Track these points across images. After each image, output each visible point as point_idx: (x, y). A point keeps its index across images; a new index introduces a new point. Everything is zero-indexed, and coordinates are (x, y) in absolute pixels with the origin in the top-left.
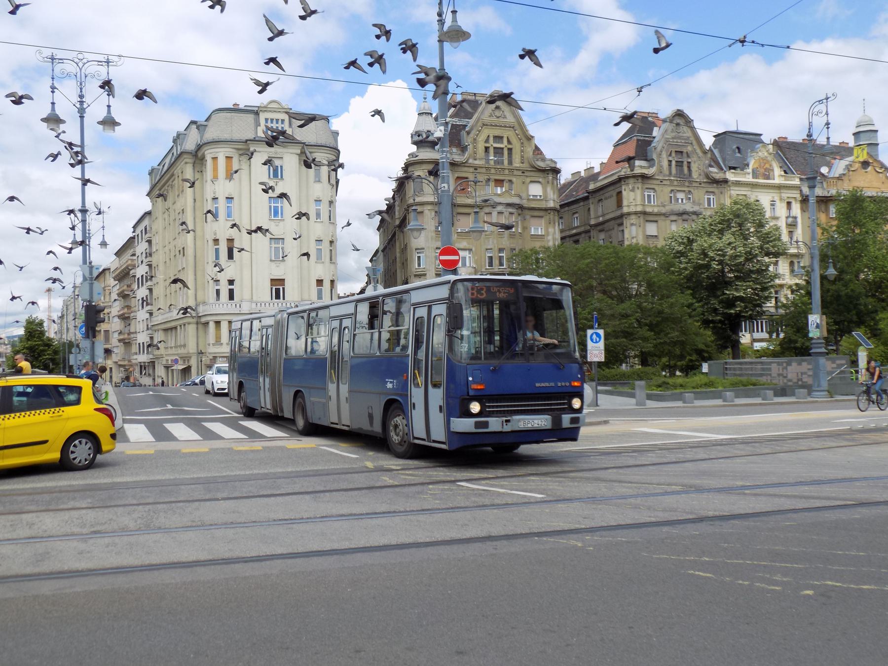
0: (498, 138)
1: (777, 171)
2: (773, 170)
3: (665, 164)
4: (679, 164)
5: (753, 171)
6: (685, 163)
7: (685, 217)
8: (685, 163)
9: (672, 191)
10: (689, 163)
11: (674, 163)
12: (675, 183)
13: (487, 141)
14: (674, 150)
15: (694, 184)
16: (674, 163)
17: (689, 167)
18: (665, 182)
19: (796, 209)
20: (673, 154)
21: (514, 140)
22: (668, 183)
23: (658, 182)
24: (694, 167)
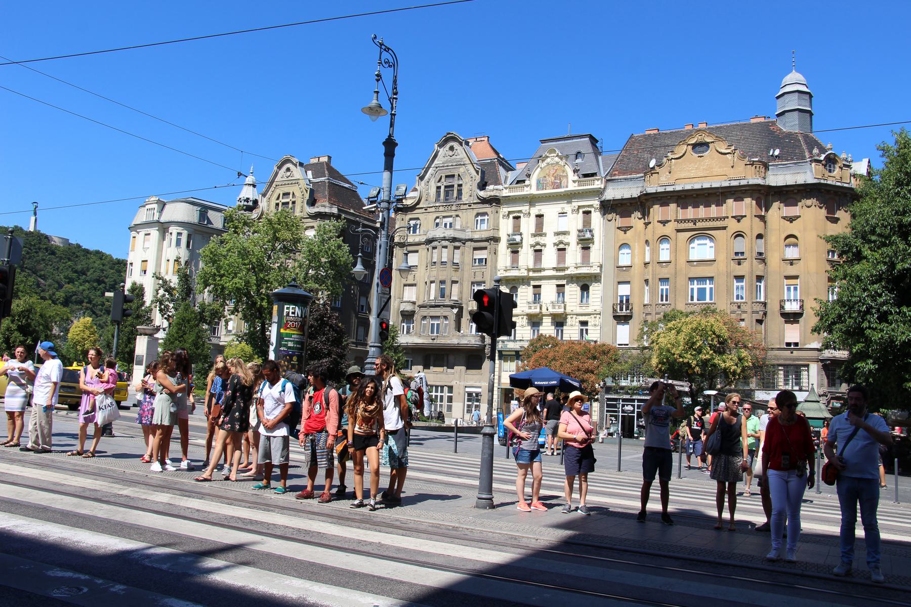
0: (286, 194)
1: (572, 176)
2: (567, 176)
3: (433, 191)
4: (449, 187)
5: (538, 182)
6: (456, 186)
7: (435, 244)
8: (456, 186)
9: (437, 217)
10: (460, 185)
11: (443, 188)
12: (441, 209)
13: (278, 198)
14: (444, 175)
15: (462, 207)
16: (443, 188)
18: (429, 210)
21: (298, 194)
23: (423, 210)
24: (465, 190)
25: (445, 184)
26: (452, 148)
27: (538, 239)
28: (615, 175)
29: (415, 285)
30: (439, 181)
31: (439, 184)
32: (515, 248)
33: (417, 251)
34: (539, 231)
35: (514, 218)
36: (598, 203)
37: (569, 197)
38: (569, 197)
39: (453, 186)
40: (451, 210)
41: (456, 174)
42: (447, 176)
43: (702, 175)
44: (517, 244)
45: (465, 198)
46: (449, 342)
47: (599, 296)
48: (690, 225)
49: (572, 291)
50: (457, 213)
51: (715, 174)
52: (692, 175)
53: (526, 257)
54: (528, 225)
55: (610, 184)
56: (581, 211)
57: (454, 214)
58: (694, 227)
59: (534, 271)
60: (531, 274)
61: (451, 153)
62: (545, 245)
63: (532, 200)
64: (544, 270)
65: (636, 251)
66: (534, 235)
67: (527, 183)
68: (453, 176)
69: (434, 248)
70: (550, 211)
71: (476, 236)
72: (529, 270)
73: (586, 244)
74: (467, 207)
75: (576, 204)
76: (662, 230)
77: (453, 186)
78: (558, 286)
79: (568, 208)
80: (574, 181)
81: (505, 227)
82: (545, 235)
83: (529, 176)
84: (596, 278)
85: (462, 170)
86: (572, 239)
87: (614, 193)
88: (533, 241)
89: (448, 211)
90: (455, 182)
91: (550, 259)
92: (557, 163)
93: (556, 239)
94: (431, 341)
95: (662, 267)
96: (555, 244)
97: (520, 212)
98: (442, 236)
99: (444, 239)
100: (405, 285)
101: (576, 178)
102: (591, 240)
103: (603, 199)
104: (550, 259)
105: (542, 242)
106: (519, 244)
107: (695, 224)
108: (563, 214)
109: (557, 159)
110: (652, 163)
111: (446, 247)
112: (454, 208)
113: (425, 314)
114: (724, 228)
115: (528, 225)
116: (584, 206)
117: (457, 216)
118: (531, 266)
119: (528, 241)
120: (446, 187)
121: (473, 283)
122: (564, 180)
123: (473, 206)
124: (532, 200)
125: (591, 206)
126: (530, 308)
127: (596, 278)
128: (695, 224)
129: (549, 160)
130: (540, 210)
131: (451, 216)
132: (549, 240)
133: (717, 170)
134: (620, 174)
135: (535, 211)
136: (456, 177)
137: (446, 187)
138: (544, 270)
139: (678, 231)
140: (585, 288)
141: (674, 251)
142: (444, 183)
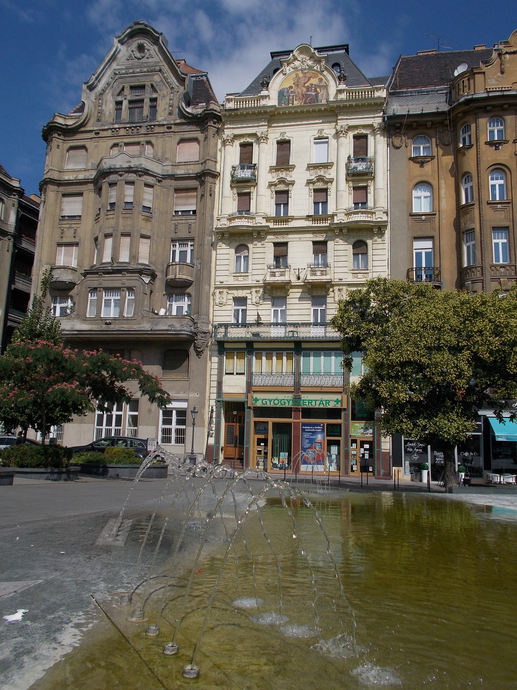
1: (333, 87)
2: (326, 87)
3: (109, 107)
5: (281, 94)
6: (147, 101)
8: (147, 101)
10: (154, 100)
11: (125, 103)
12: (122, 132)
15: (157, 130)
16: (125, 103)
17: (153, 108)
18: (102, 134)
19: (379, 147)
20: (127, 91)
22: (109, 133)
23: (93, 135)
24: (162, 106)
25: (129, 98)
26: (141, 48)
27: (283, 175)
29: (77, 244)
30: (118, 95)
31: (119, 99)
32: (244, 187)
33: (80, 194)
34: (283, 163)
35: (242, 145)
36: (380, 120)
37: (331, 112)
39: (142, 101)
40: (139, 134)
41: (148, 84)
42: (132, 88)
45: (161, 117)
46: (136, 327)
47: (386, 258)
49: (340, 250)
50: (147, 139)
53: (263, 203)
56: (351, 134)
57: (142, 139)
59: (276, 220)
60: (271, 225)
61: (138, 55)
62: (292, 183)
64: (293, 218)
66: (273, 169)
68: (143, 87)
69: (112, 184)
70: (302, 136)
71: (180, 171)
73: (360, 180)
74: (165, 129)
75: (344, 122)
76: (490, 156)
77: (142, 101)
78: (315, 243)
79: (329, 129)
81: (228, 158)
82: (293, 167)
84: (378, 229)
85: (157, 78)
86: (338, 175)
88: (274, 178)
89: (132, 136)
90: (147, 96)
91: (301, 203)
92: (311, 68)
93: (312, 175)
94: (104, 327)
95: (496, 210)
96: (309, 182)
97: (255, 135)
98: (126, 165)
99: (129, 170)
100: (60, 245)
102: (369, 175)
103: (390, 113)
104: (301, 203)
105: (289, 179)
106: (252, 181)
108: (321, 139)
109: (310, 63)
111: (132, 183)
112: (143, 131)
113: (95, 284)
115: (265, 155)
116: (356, 127)
117: (149, 143)
118: (272, 212)
119: (265, 177)
120: (130, 102)
121: (173, 241)
122: (321, 93)
123: (174, 128)
124: (272, 116)
125: (371, 126)
126: (273, 274)
127: (378, 229)
129: (297, 63)
130: (283, 134)
131: (138, 143)
132: (300, 176)
136: (148, 89)
137: (130, 102)
138: (293, 218)
140: (360, 248)
142: (129, 95)
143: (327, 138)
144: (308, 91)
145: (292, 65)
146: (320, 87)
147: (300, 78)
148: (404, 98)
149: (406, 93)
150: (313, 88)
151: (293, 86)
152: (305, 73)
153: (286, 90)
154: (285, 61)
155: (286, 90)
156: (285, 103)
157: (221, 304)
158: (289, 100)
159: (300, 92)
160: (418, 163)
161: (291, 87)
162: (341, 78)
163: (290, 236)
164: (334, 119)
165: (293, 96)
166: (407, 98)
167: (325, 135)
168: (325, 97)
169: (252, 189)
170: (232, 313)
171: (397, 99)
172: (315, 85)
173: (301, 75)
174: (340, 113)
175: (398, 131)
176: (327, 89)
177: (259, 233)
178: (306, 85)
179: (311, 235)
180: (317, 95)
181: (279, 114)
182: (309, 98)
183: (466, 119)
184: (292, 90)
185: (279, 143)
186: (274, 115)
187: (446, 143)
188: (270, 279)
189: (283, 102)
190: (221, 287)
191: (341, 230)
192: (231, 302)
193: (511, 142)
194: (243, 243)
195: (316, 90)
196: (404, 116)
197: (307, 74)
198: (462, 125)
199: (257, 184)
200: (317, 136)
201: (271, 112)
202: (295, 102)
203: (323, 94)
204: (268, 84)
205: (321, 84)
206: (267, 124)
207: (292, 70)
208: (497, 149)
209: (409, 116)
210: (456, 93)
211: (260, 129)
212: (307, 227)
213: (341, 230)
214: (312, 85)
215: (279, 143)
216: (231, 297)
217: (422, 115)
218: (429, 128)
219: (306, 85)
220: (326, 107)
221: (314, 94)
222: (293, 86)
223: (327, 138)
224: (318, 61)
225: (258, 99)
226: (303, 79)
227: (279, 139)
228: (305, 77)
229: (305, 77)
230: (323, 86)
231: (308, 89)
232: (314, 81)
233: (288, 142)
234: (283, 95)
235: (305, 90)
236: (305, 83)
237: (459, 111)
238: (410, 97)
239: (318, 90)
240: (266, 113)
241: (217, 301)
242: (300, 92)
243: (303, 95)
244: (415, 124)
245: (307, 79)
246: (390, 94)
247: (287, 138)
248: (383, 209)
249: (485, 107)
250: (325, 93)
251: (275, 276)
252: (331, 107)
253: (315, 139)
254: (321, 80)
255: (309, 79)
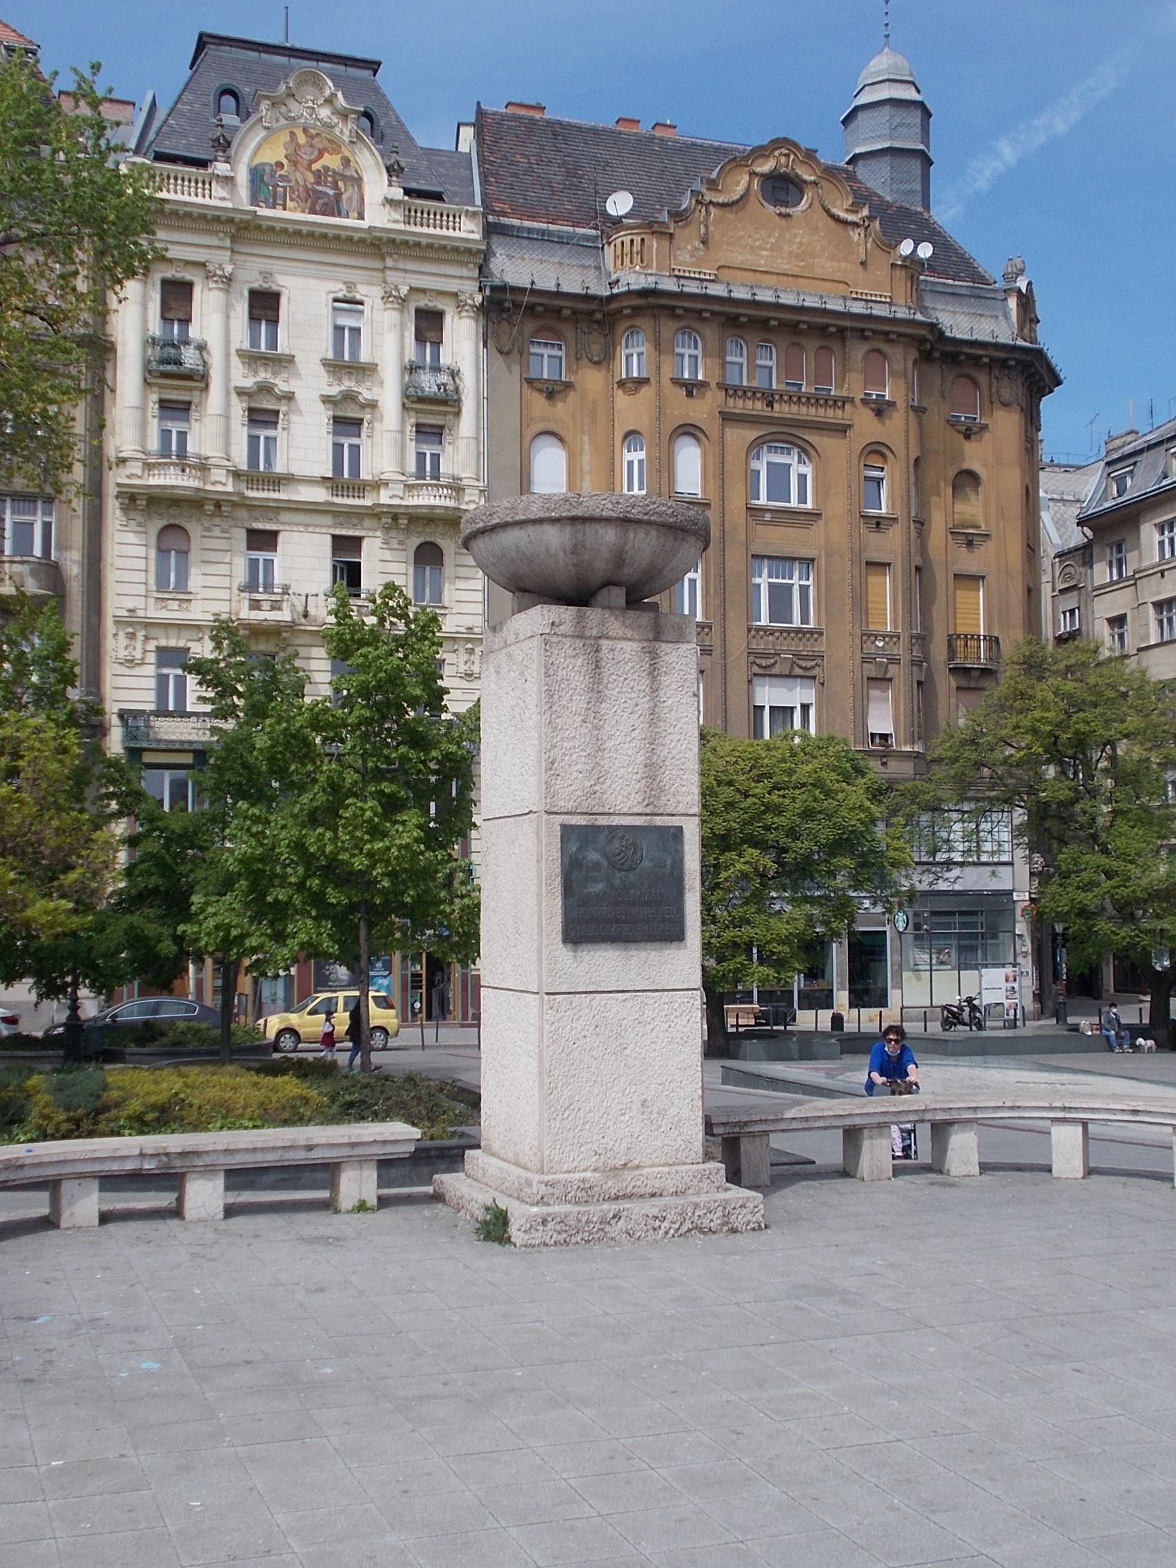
2: (358, 181)
5: (257, 175)
19: (461, 339)
28: (505, 214)
38: (378, 247)
43: (784, 266)
44: (188, 377)
48: (759, 407)
51: (818, 272)
52: (762, 264)
53: (216, 433)
54: (216, 321)
55: (495, 239)
58: (767, 412)
62: (289, 397)
63: (241, 231)
65: (586, 459)
67: (221, 168)
72: (237, 474)
73: (431, 413)
80: (390, 202)
83: (223, 145)
86: (387, 393)
87: (518, 268)
91: (305, 446)
96: (326, 400)
101: (398, 193)
102: (449, 402)
104: (305, 446)
107: (770, 404)
110: (620, 204)
114: (842, 430)
119: (227, 376)
122: (348, 193)
124: (241, 231)
128: (770, 404)
133: (825, 265)
134: (516, 213)
135: (252, 271)
139: (728, 418)
141: (716, 471)
143: (361, 303)
144: (319, 184)
145: (283, 109)
146: (344, 177)
147: (299, 146)
148: (515, 240)
149: (520, 229)
150: (330, 179)
151: (285, 162)
152: (312, 137)
153: (268, 169)
154: (267, 98)
155: (268, 169)
156: (266, 202)
157: (130, 662)
158: (275, 196)
159: (301, 182)
160: (541, 391)
161: (280, 165)
162: (393, 171)
163: (285, 516)
164: (377, 264)
165: (285, 188)
166: (521, 241)
167: (358, 297)
168: (355, 204)
169: (195, 397)
170: (152, 683)
171: (502, 238)
172: (334, 172)
173: (302, 139)
174: (391, 255)
175: (505, 315)
176: (360, 188)
177: (218, 505)
178: (315, 167)
179: (328, 520)
180: (338, 197)
181: (259, 227)
182: (321, 201)
183: (637, 322)
184: (283, 172)
185: (253, 293)
186: (246, 229)
187: (596, 359)
188: (246, 614)
189: (262, 197)
190: (133, 624)
191: (395, 517)
192: (152, 658)
193: (713, 385)
194: (177, 522)
195: (335, 187)
196: (522, 290)
197: (316, 140)
198: (628, 328)
199: (207, 386)
200: (340, 295)
201: (242, 221)
202: (289, 204)
203: (350, 198)
204: (229, 144)
205: (348, 173)
206: (228, 243)
207: (283, 121)
208: (690, 394)
209: (533, 292)
210: (616, 257)
211: (221, 260)
212: (327, 503)
213: (395, 517)
214: (326, 169)
215: (253, 293)
216: (152, 646)
217: (558, 294)
218: (566, 319)
219: (315, 167)
220: (363, 235)
221: (331, 192)
222: (285, 162)
223: (361, 303)
224: (344, 115)
225: (207, 180)
226: (308, 150)
227: (256, 285)
228: (312, 146)
229: (312, 146)
230: (352, 179)
231: (317, 174)
232: (331, 161)
233: (276, 296)
234: (262, 180)
235: (311, 178)
236: (311, 162)
237: (625, 303)
238: (527, 242)
239: (341, 184)
240: (231, 221)
241: (122, 654)
242: (301, 182)
243: (307, 190)
244: (539, 309)
245: (316, 152)
246: (490, 230)
247: (275, 288)
248: (477, 484)
249: (673, 308)
250: (356, 197)
251: (259, 609)
252: (375, 238)
253: (336, 300)
254: (346, 162)
255: (320, 156)
